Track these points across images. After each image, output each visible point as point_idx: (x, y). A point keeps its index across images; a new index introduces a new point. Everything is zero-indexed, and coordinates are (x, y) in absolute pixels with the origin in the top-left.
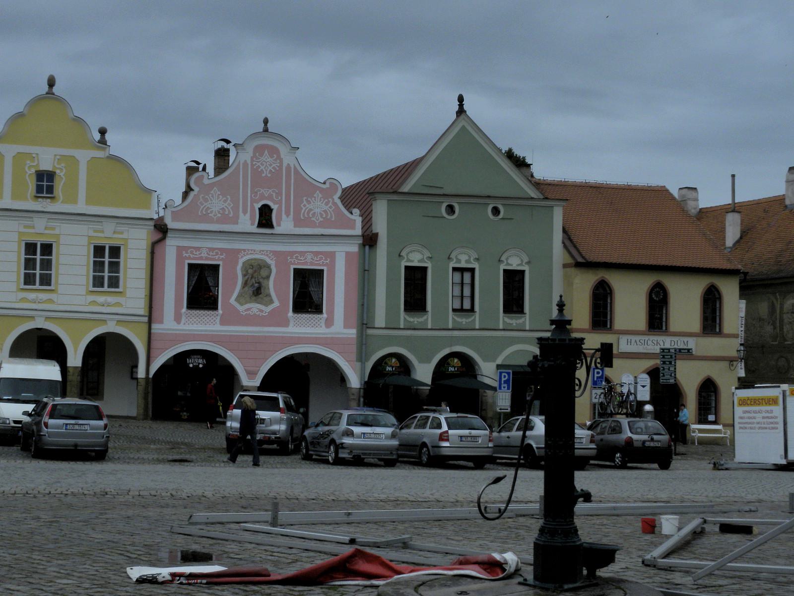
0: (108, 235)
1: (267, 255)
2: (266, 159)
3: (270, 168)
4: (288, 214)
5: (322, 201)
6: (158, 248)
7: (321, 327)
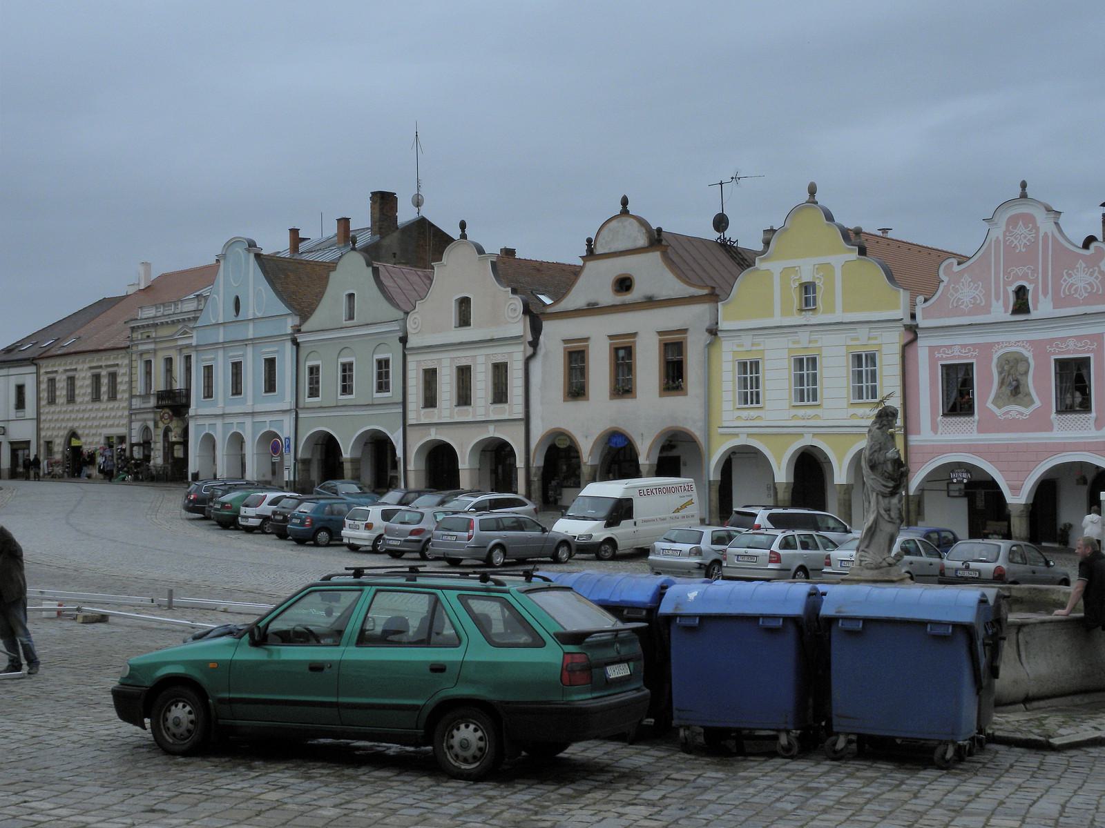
0: (862, 341)
1: (1024, 346)
3: (1025, 241)
4: (1045, 293)
6: (910, 351)
7: (1090, 429)
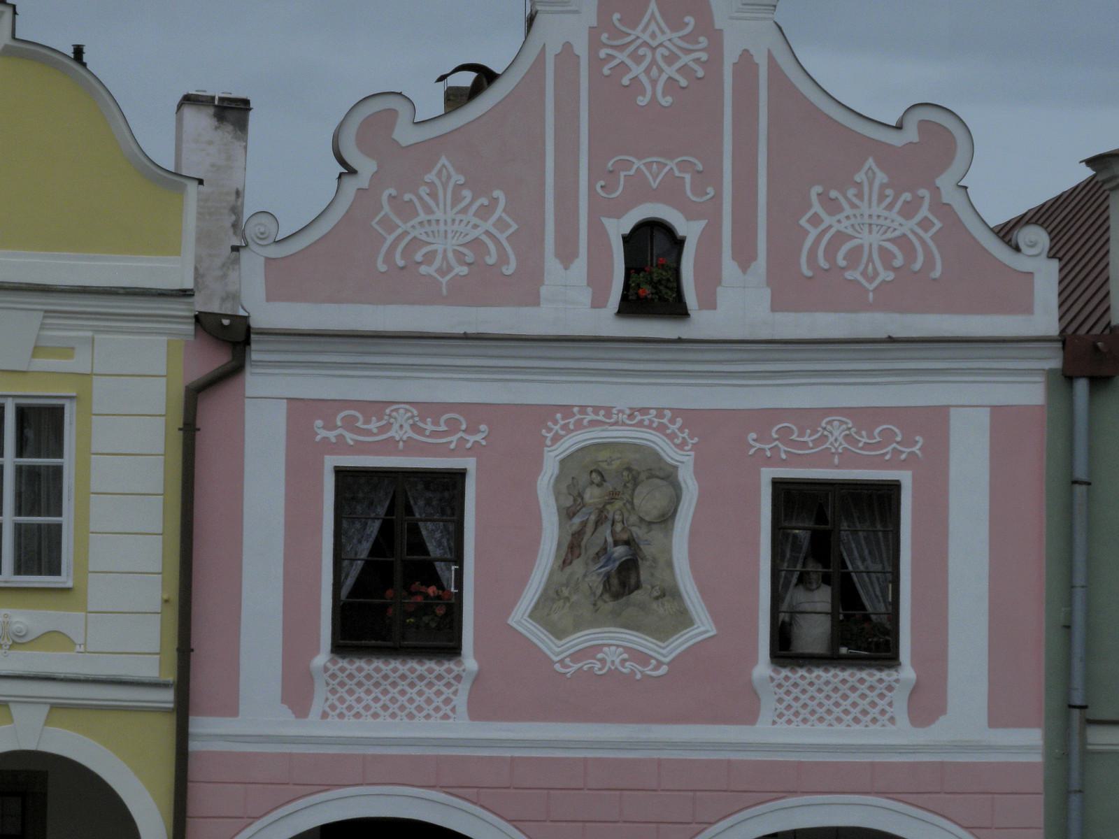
1: (661, 428)
2: (653, 36)
3: (670, 71)
5: (889, 200)
6: (212, 412)
7: (892, 720)
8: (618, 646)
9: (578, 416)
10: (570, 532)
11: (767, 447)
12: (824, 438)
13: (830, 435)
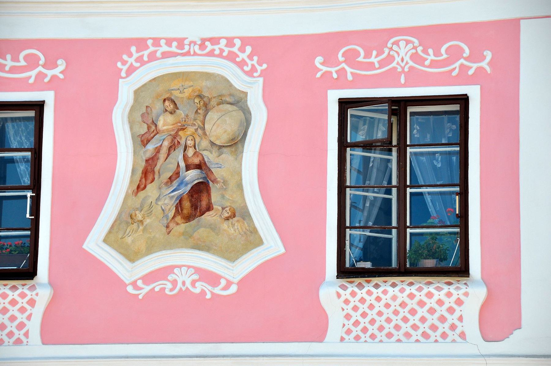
1: (231, 57)
8: (189, 267)
9: (152, 49)
10: (144, 158)
11: (333, 70)
12: (390, 59)
13: (396, 55)
